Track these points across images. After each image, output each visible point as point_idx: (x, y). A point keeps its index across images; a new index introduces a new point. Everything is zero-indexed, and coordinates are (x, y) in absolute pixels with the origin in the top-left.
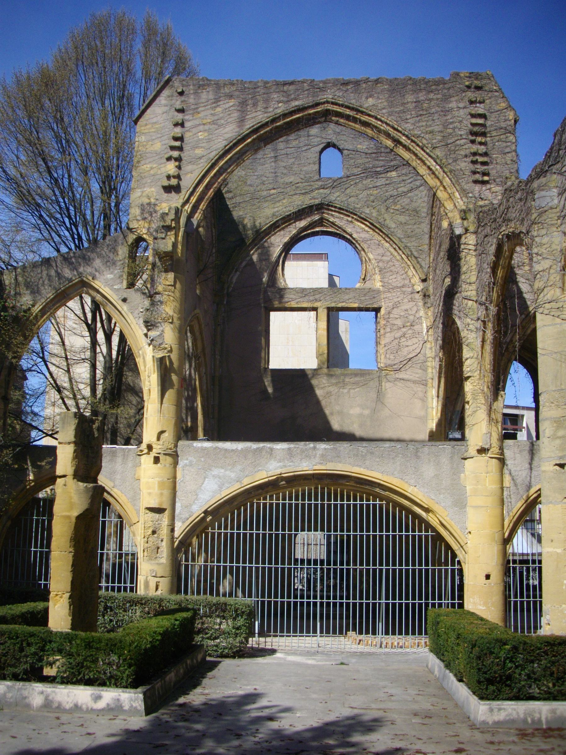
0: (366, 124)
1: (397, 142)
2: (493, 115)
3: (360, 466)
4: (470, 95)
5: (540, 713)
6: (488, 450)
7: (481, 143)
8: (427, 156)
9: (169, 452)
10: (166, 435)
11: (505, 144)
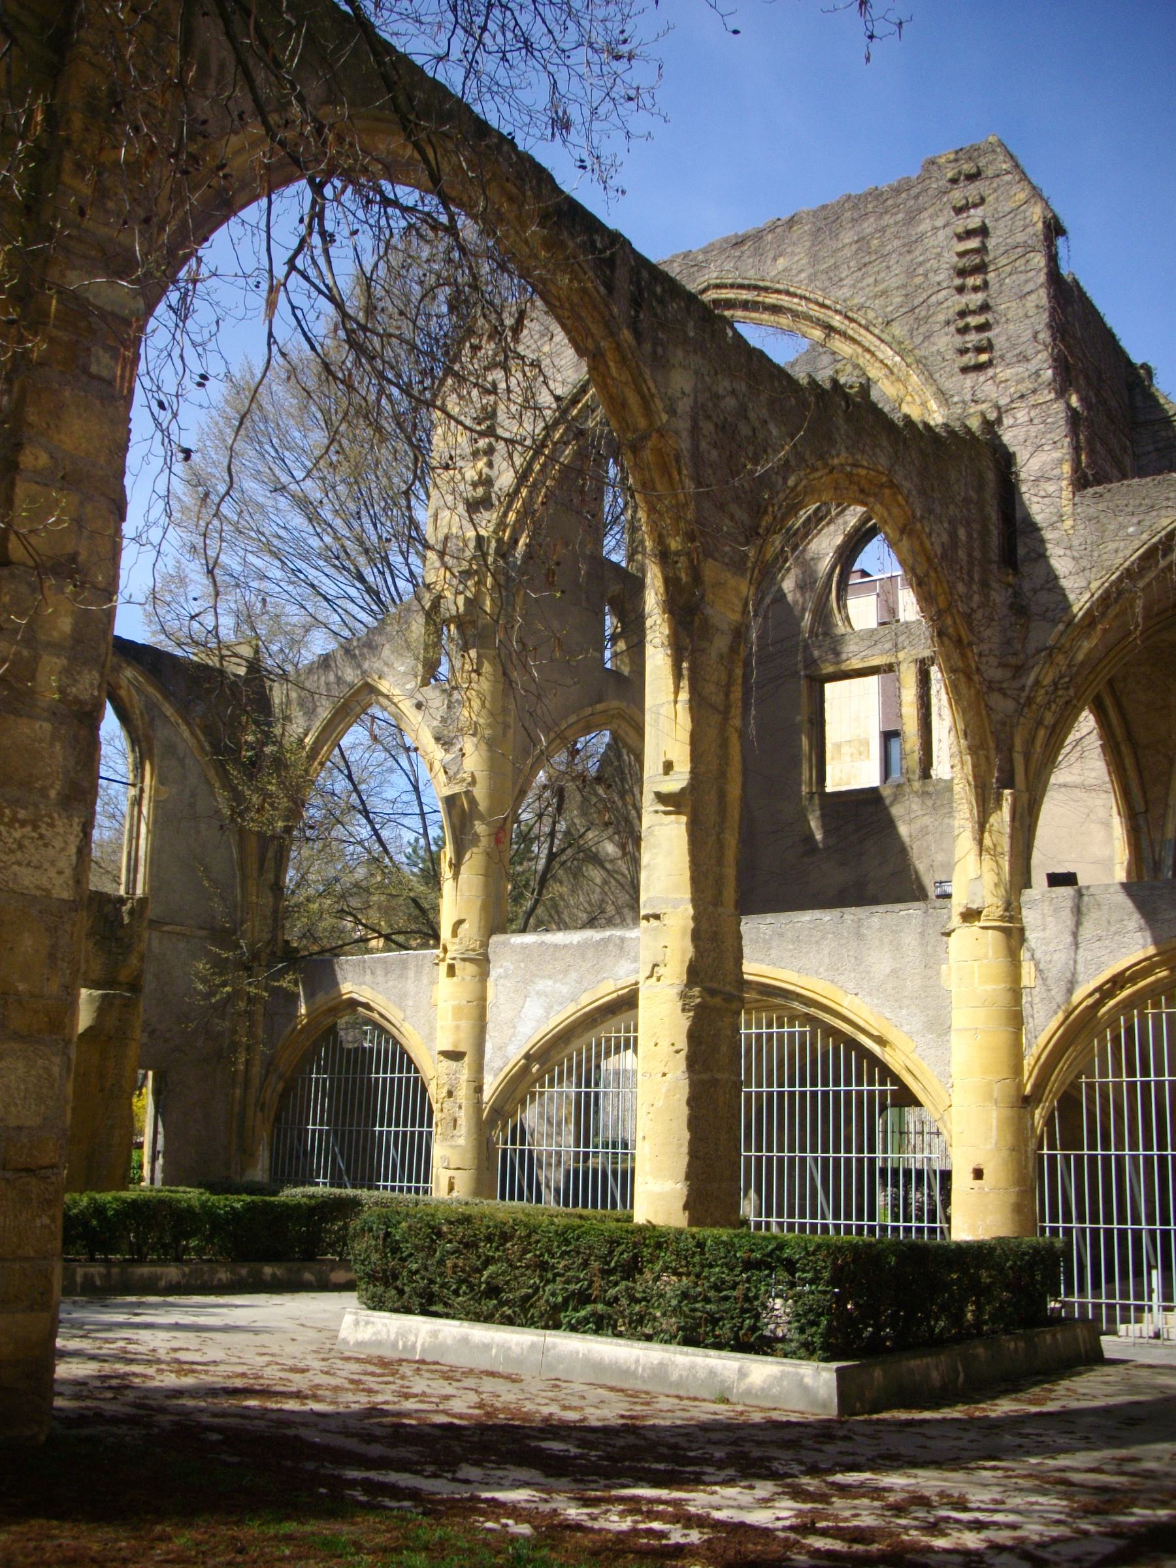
0: (776, 309)
1: (829, 329)
2: (1001, 224)
3: (761, 961)
4: (957, 196)
5: (416, 1336)
6: (980, 913)
7: (976, 289)
8: (878, 343)
9: (471, 955)
10: (465, 926)
11: (1023, 277)
